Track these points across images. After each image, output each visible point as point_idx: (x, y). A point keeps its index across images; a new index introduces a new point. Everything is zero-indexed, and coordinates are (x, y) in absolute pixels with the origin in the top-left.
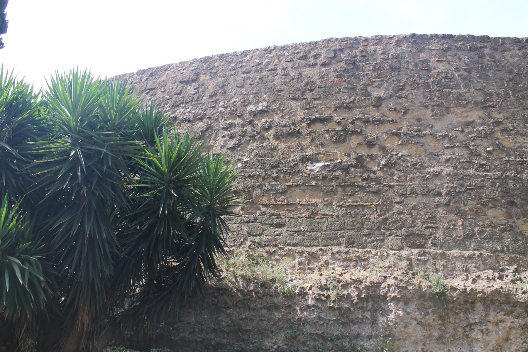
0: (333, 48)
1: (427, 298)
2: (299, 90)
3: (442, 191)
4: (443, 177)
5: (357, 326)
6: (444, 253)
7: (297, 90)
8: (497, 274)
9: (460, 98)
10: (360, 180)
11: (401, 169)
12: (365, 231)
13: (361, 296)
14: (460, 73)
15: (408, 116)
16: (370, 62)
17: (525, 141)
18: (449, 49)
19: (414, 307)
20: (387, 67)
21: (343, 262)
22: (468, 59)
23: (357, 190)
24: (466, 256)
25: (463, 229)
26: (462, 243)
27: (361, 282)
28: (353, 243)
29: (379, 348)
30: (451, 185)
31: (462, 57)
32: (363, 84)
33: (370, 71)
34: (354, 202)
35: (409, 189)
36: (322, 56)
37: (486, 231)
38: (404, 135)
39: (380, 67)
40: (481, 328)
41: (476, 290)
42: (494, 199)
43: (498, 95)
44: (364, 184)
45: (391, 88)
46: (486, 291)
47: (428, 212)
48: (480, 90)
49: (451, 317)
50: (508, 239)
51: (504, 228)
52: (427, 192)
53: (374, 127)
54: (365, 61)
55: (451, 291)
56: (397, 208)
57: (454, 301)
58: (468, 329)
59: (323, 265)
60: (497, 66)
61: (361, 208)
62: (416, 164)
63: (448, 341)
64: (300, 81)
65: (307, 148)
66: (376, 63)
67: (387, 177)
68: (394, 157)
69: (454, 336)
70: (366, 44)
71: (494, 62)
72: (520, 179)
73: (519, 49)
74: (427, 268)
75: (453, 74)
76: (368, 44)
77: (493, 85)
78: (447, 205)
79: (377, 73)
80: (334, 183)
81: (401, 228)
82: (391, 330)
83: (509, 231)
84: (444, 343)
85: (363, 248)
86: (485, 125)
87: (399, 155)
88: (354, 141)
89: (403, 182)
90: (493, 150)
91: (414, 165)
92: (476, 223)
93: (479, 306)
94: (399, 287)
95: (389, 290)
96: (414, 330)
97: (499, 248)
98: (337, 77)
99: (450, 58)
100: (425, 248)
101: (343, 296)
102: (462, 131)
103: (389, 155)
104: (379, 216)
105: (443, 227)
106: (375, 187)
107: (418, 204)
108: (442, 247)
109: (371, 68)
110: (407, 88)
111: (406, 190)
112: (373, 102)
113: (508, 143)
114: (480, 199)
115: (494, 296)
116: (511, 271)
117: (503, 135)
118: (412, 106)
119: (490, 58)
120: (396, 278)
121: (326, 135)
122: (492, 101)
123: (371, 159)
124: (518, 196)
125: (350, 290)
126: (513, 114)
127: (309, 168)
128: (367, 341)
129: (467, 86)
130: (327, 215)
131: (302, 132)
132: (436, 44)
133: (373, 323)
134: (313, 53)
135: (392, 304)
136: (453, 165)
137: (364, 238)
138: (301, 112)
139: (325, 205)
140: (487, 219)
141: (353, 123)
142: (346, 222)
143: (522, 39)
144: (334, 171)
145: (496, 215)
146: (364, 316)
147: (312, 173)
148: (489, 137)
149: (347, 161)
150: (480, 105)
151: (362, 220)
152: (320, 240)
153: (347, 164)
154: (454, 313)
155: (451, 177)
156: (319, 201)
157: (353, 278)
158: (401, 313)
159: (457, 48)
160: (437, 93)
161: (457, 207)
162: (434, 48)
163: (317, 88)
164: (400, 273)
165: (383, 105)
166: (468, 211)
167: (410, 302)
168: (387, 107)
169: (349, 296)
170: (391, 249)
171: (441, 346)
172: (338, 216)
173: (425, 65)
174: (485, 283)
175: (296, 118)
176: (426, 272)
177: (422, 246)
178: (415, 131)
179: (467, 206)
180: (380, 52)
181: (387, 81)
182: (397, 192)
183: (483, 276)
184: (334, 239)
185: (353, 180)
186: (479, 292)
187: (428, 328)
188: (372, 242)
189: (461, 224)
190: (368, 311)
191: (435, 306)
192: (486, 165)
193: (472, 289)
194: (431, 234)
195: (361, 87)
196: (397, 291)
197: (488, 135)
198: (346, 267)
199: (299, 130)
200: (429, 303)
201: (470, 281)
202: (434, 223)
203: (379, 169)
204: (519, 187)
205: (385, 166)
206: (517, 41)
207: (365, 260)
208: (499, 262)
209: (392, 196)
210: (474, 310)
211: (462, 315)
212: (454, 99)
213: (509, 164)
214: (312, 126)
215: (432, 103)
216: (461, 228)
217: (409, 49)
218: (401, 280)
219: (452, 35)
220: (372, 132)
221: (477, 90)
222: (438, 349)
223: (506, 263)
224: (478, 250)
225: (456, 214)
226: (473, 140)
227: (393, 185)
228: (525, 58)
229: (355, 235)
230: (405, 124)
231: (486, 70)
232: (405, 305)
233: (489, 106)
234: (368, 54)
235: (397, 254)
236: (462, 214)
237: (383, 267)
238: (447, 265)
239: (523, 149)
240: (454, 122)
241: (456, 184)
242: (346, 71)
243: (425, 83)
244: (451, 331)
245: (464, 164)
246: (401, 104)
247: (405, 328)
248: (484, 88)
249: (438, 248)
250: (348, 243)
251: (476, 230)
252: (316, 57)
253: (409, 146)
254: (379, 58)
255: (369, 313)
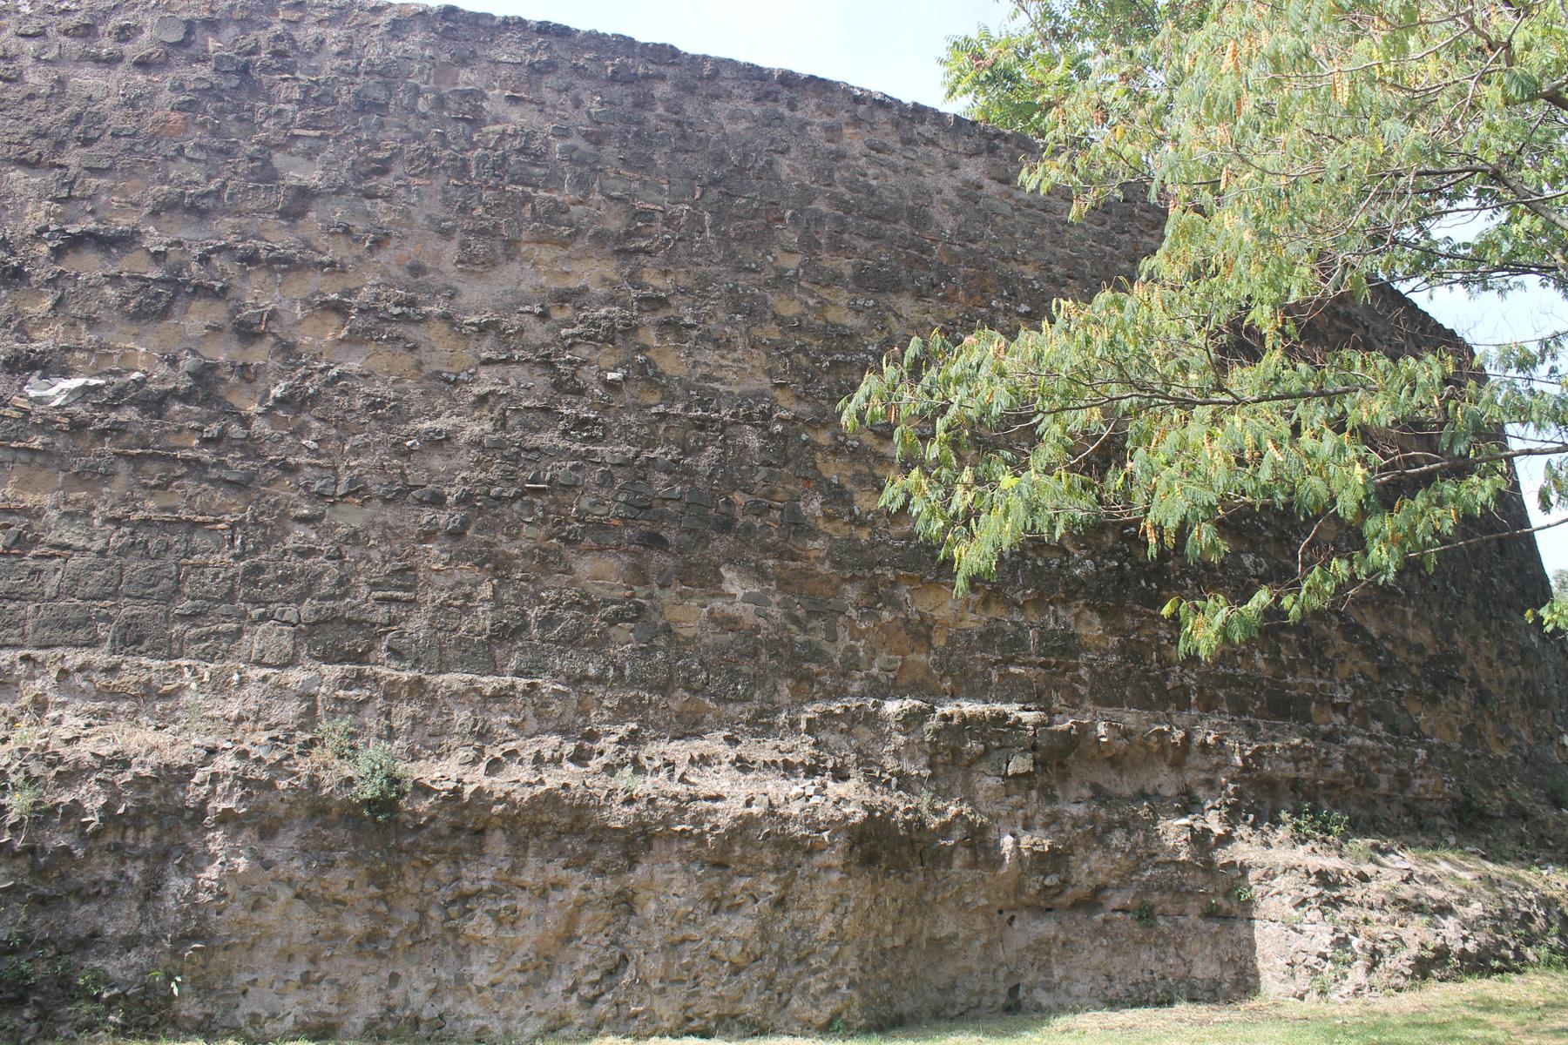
0: (186, 16)
1: (333, 816)
2: (44, 136)
3: (446, 490)
4: (458, 449)
5: (94, 907)
6: (420, 681)
7: (39, 134)
8: (569, 748)
9: (556, 216)
10: (196, 442)
11: (332, 415)
12: (185, 606)
13: (117, 808)
14: (569, 142)
15: (384, 256)
16: (298, 74)
17: (725, 363)
18: (550, 67)
19: (291, 844)
20: (345, 98)
21: (96, 699)
22: (602, 104)
23: (179, 472)
24: (488, 691)
25: (492, 610)
26: (483, 654)
27: (126, 764)
28: (139, 641)
29: (159, 977)
30: (479, 475)
31: (584, 96)
32: (258, 142)
33: (290, 101)
34: (164, 509)
35: (344, 479)
36: (146, 35)
37: (562, 620)
38: (361, 311)
39: (326, 94)
40: (495, 908)
41: (491, 793)
42: (600, 523)
43: (669, 221)
44: (206, 455)
45: (348, 163)
46: (516, 796)
47: (393, 554)
48: (619, 199)
49: (410, 873)
50: (624, 641)
51: (616, 613)
52: (399, 491)
53: (269, 280)
54: (281, 70)
55: (414, 796)
56: (299, 534)
57: (419, 828)
58: (453, 911)
59: (23, 710)
60: (684, 137)
61: (181, 529)
62: (382, 405)
63: (393, 948)
64: (54, 107)
65: (38, 327)
66: (316, 82)
67: (282, 438)
68: (317, 376)
69: (418, 931)
70: (296, 15)
71: (679, 124)
72: (690, 472)
73: (757, 100)
74: (363, 726)
75: (547, 144)
76: (301, 19)
77: (661, 191)
78: (456, 534)
79: (310, 112)
80: (108, 447)
81: (300, 599)
82: (205, 918)
83: (631, 620)
84: (381, 956)
85: (170, 657)
86: (614, 304)
87: (334, 372)
88: (196, 319)
89: (329, 455)
90: (625, 378)
91: (374, 406)
92: (536, 595)
93: (497, 842)
94: (246, 782)
95: (214, 791)
96: (285, 915)
97: (592, 671)
98: (179, 108)
99: (548, 95)
100: (368, 663)
101: (52, 811)
102: (544, 316)
103: (301, 371)
104: (237, 557)
105: (433, 600)
106: (237, 465)
107: (366, 529)
108: (418, 661)
109: (297, 95)
110: (398, 168)
111: (336, 483)
112: (281, 199)
113: (672, 363)
114: (559, 523)
115: (540, 811)
116: (614, 738)
117: (661, 338)
118: (403, 225)
119: (667, 110)
120: (243, 755)
121: (109, 291)
122: (650, 236)
123: (242, 377)
124: (674, 520)
125: (83, 791)
126: (704, 282)
127: (33, 394)
128: (120, 954)
129: (582, 183)
130: (68, 547)
131: (29, 274)
132: (513, 48)
133: (147, 897)
134: (117, 20)
135: (219, 834)
136: (496, 413)
137: (178, 627)
138: (39, 209)
139: (65, 514)
140: (573, 582)
141: (204, 259)
142: (127, 572)
143: (771, 71)
144: (115, 408)
145: (599, 572)
146: (122, 875)
147: (38, 409)
148: (619, 342)
149: (162, 378)
150: (610, 243)
151: (179, 567)
152: (29, 627)
153: (161, 387)
154: (419, 864)
155: (484, 450)
156: (48, 500)
157: (105, 750)
158: (242, 863)
159: (576, 68)
160: (487, 195)
161: (486, 543)
162: (505, 58)
163: (107, 137)
164: (264, 737)
165: (312, 215)
166: (517, 557)
167: (282, 830)
168: (322, 221)
169: (75, 808)
170: (260, 663)
171: (371, 963)
172: (102, 553)
173: (466, 107)
174: (525, 773)
175: (20, 227)
176: (353, 735)
177: (360, 659)
178: (397, 304)
179: (518, 543)
180: (335, 49)
181: (337, 140)
182: (306, 487)
183: (524, 754)
184: (77, 626)
185: (173, 441)
186: (499, 801)
187: (330, 911)
188: (199, 639)
189: (488, 593)
190: (137, 858)
191: (356, 842)
192: (594, 422)
193: (479, 792)
194: (392, 621)
195: (250, 149)
196: (238, 793)
197: (610, 336)
198: (104, 715)
199: (23, 264)
200: (342, 833)
201: (482, 766)
202: (406, 589)
203: (261, 410)
204: (681, 492)
205: (281, 402)
206: (753, 74)
207: (167, 696)
208: (586, 713)
209: (289, 498)
210: (483, 855)
211: (442, 869)
212: (535, 216)
213: (663, 426)
214: (68, 258)
215: (467, 224)
216: (487, 606)
217: (428, 53)
218: (259, 761)
219: (567, 28)
220: (258, 294)
221: (612, 198)
222: (358, 972)
223: (607, 715)
224: (528, 675)
225: (480, 565)
226: (571, 346)
227: (298, 465)
228: (769, 125)
229: (146, 617)
230: (372, 279)
231: (649, 144)
232: (262, 838)
233: (638, 250)
234: (295, 47)
235: (273, 680)
236: (498, 566)
237: (215, 720)
238: (425, 717)
239: (716, 385)
240: (523, 287)
241: (494, 473)
242: (212, 92)
243: (455, 159)
244: (408, 917)
245: (531, 415)
246: (368, 215)
247: (253, 909)
248: (633, 196)
249: (408, 664)
250: (123, 640)
251: (533, 613)
252: (125, 34)
253: (372, 347)
254: (329, 66)
255: (141, 865)
